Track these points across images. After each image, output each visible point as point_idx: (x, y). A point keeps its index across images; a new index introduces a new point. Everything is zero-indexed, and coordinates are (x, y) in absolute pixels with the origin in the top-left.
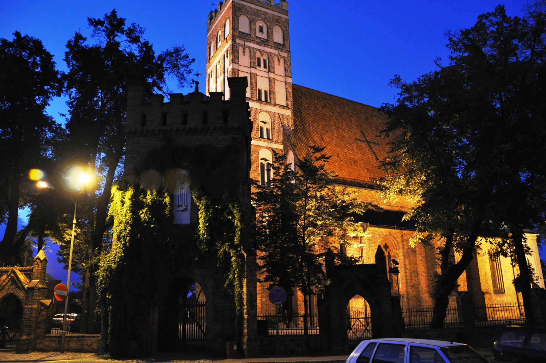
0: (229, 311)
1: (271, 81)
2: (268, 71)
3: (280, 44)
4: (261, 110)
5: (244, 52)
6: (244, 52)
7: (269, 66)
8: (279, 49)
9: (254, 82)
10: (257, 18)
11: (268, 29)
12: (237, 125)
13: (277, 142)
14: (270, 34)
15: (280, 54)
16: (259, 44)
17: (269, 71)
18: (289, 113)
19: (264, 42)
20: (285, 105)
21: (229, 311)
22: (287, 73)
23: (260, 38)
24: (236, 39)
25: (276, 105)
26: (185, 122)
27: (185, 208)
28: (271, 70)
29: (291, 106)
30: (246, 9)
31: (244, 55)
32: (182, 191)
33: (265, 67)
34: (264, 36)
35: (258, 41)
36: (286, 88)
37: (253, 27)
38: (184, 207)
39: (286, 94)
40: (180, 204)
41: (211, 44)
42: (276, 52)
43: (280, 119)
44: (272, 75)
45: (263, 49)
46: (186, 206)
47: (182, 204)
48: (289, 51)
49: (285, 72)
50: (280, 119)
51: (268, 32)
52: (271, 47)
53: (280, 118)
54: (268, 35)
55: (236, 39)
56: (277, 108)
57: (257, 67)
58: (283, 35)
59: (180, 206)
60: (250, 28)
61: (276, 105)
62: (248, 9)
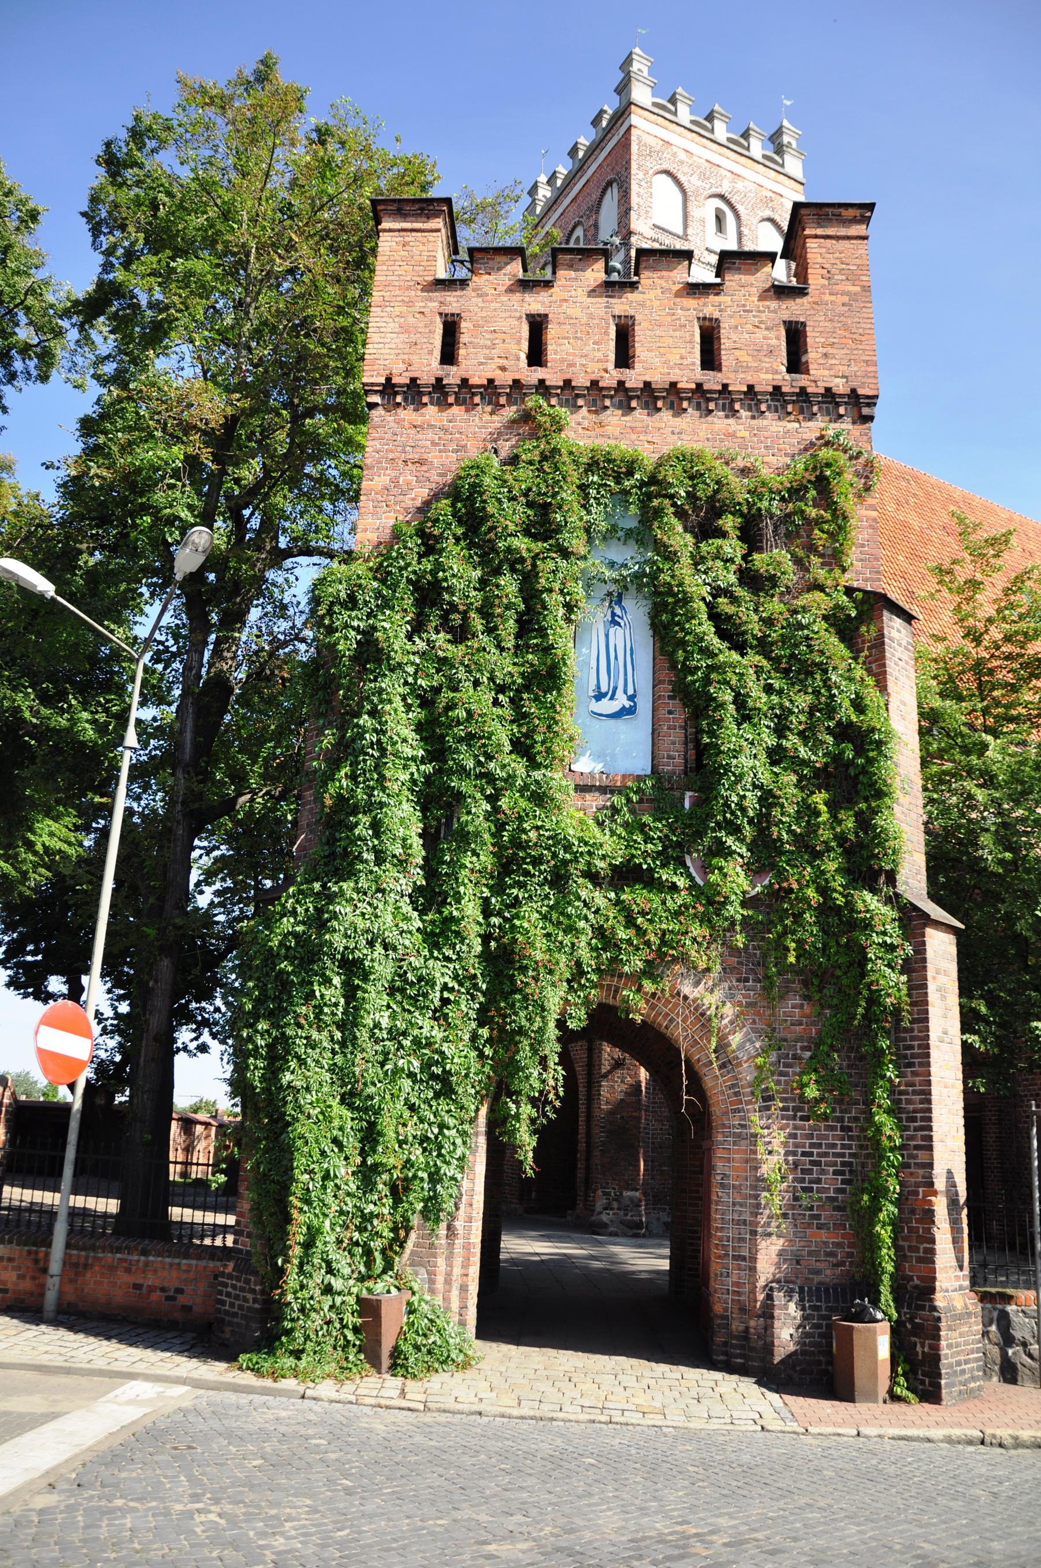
0: (835, 1173)
21: (835, 1173)
26: (624, 357)
27: (628, 704)
30: (674, 155)
32: (612, 631)
38: (621, 701)
40: (604, 689)
46: (631, 698)
47: (615, 689)
59: (605, 695)
62: (682, 156)
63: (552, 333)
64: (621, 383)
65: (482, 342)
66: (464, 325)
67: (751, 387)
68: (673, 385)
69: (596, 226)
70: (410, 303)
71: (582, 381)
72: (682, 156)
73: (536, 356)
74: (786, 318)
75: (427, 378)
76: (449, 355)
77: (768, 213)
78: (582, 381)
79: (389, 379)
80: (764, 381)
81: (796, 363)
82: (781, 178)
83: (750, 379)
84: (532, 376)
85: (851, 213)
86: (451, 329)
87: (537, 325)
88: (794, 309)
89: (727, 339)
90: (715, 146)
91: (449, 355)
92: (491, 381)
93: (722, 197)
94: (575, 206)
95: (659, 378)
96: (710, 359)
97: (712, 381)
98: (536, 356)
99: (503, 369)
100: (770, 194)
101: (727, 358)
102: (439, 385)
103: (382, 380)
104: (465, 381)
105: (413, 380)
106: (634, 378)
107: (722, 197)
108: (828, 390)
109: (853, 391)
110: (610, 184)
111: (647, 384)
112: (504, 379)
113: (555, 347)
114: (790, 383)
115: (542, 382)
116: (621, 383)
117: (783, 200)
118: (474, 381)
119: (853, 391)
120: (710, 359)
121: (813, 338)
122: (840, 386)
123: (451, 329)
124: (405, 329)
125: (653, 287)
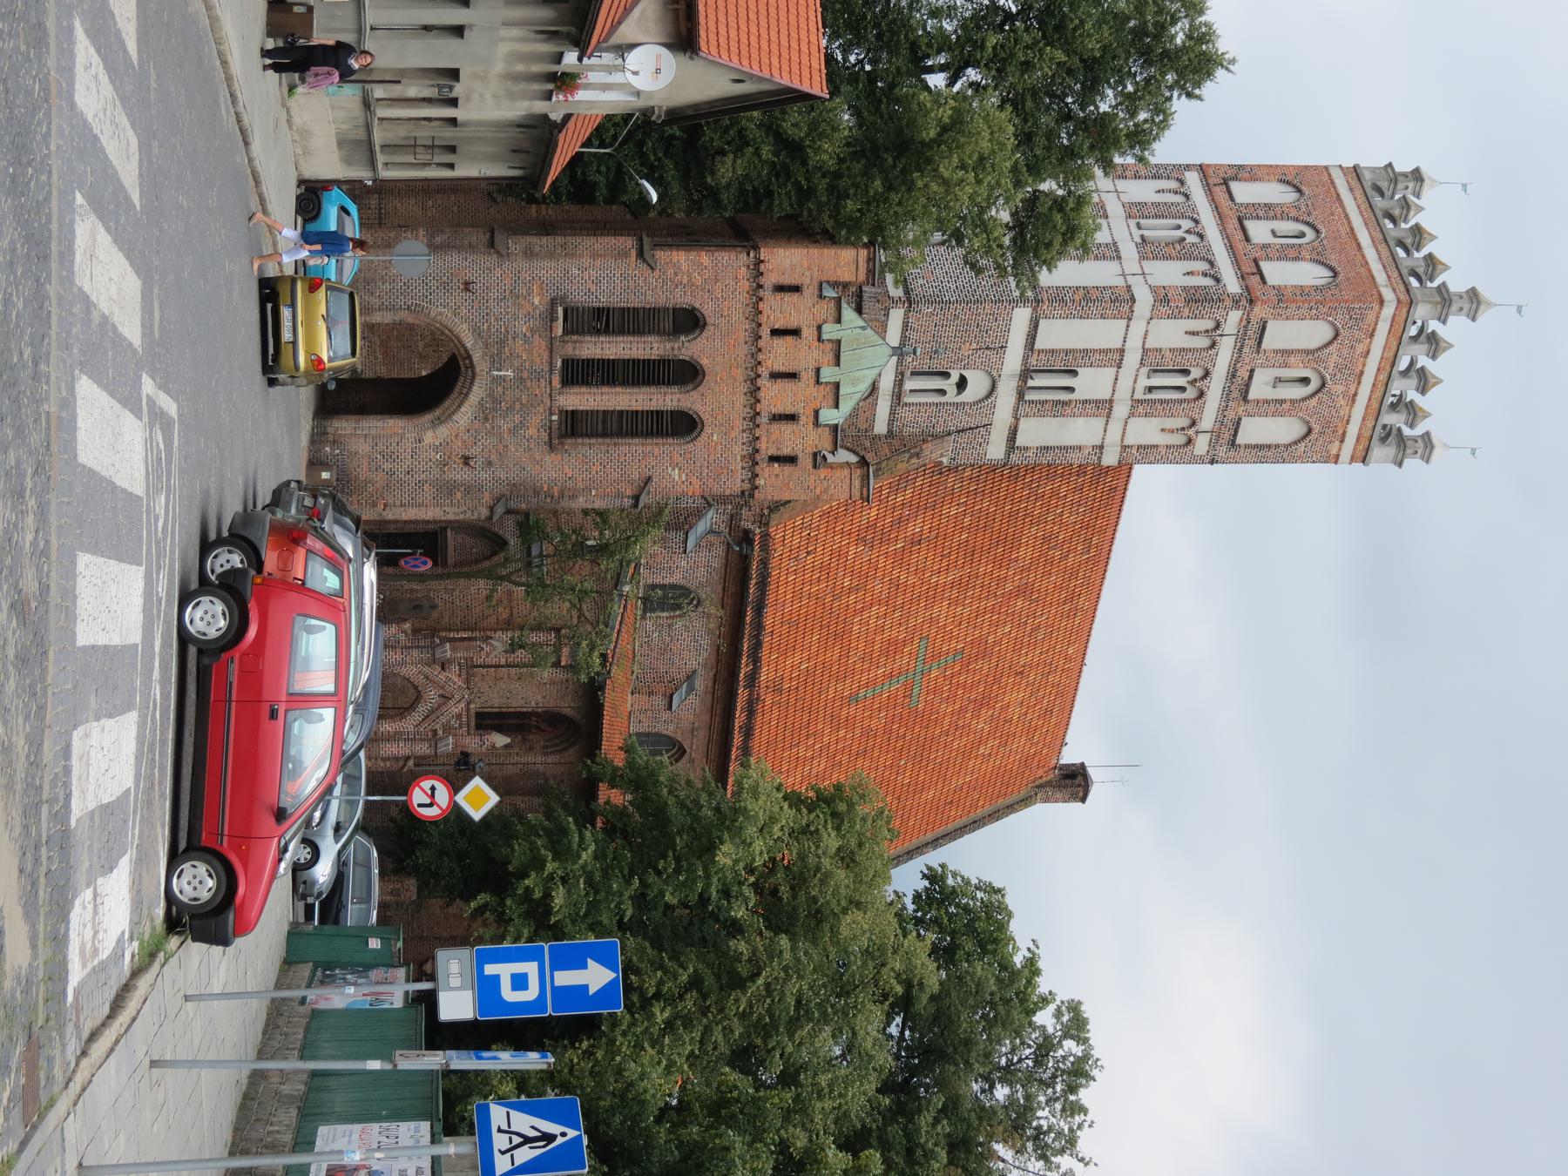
1: (1104, 407)
2: (1137, 396)
3: (1235, 435)
4: (1000, 376)
5: (1193, 333)
6: (1193, 333)
7: (1154, 402)
8: (1216, 435)
9: (1092, 359)
10: (1330, 371)
11: (1292, 401)
12: (762, 482)
13: (891, 421)
14: (1276, 407)
15: (1200, 435)
16: (1232, 375)
17: (1136, 403)
18: (996, 450)
19: (1239, 387)
20: (1020, 442)
22: (1134, 451)
23: (1251, 377)
24: (1240, 312)
25: (1017, 419)
26: (775, 376)
28: (1142, 406)
29: (1014, 458)
30: (1360, 341)
31: (1186, 333)
33: (1150, 389)
34: (1259, 390)
35: (1243, 373)
36: (1080, 448)
37: (1292, 359)
39: (1060, 448)
41: (1294, 186)
42: (1208, 421)
43: (970, 429)
44: (1121, 410)
45: (1212, 386)
48: (1212, 462)
49: (1139, 447)
50: (970, 429)
51: (1282, 402)
52: (1223, 410)
53: (977, 427)
54: (1267, 402)
55: (1240, 312)
56: (1009, 420)
57: (1145, 370)
58: (1277, 446)
60: (1286, 353)
61: (1017, 419)
62: (1360, 348)
63: (789, 339)
64: (759, 376)
65: (784, 306)
66: (795, 297)
67: (758, 438)
68: (759, 401)
69: (1296, 259)
70: (809, 268)
71: (761, 357)
72: (1360, 348)
73: (776, 333)
74: (800, 456)
75: (762, 280)
76: (780, 289)
77: (1316, 428)
78: (761, 357)
79: (762, 261)
80: (762, 445)
81: (773, 459)
82: (1364, 443)
83: (764, 439)
84: (765, 332)
85: (865, 493)
86: (796, 289)
87: (795, 332)
88: (805, 461)
89: (787, 428)
90: (1383, 377)
91: (780, 289)
92: (761, 312)
93: (1323, 385)
94: (1344, 230)
95: (761, 394)
96: (778, 418)
97: (763, 420)
98: (776, 333)
99: (768, 317)
100: (1341, 432)
101: (775, 427)
102: (760, 287)
103: (762, 258)
104: (761, 299)
105: (762, 274)
106: (763, 382)
107: (1323, 385)
108: (757, 475)
109: (757, 488)
110: (1336, 274)
111: (759, 389)
112: (763, 319)
113: (781, 344)
114: (762, 456)
115: (760, 337)
116: (759, 376)
117: (1337, 443)
118: (761, 304)
119: (757, 488)
120: (778, 418)
121: (788, 469)
122: (761, 482)
123: (796, 289)
124: (793, 267)
125: (818, 391)
